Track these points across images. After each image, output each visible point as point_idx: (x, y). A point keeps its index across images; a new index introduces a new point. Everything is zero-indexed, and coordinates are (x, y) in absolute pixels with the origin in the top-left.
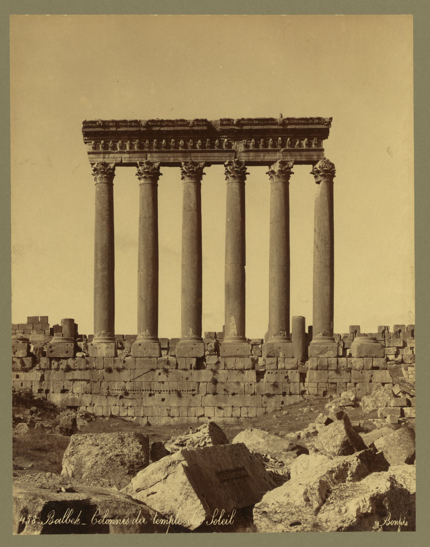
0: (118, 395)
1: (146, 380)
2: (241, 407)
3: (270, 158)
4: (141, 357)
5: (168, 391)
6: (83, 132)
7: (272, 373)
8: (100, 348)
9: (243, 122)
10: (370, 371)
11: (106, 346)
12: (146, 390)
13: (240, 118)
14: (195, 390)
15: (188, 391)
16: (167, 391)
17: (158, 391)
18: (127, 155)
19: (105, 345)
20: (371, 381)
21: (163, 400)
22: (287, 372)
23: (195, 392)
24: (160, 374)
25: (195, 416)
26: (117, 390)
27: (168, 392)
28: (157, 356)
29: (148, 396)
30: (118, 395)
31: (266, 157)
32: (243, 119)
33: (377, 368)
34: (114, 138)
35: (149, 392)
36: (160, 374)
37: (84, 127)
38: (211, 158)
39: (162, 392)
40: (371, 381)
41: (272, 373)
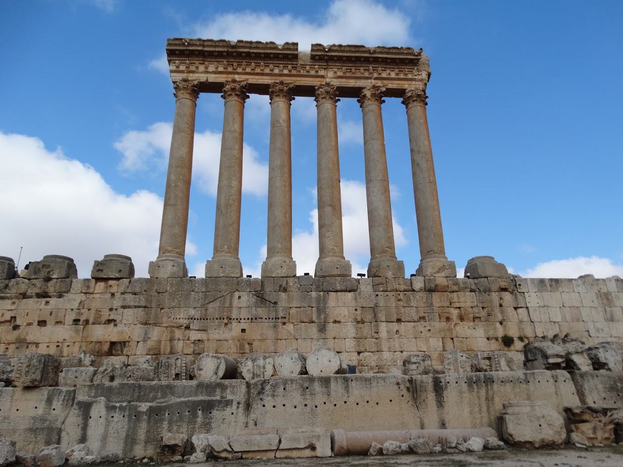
0: (182, 326)
2: (345, 339)
3: (361, 84)
5: (250, 318)
6: (167, 50)
8: (163, 266)
9: (335, 48)
10: (497, 293)
12: (220, 319)
13: (331, 44)
14: (285, 318)
15: (276, 318)
16: (248, 319)
17: (237, 319)
18: (212, 76)
19: (171, 263)
20: (501, 305)
21: (243, 331)
22: (399, 295)
23: (286, 320)
24: (239, 297)
26: (183, 318)
27: (250, 320)
28: (237, 276)
29: (223, 326)
30: (182, 326)
32: (334, 45)
33: (504, 290)
34: (200, 60)
36: (239, 297)
37: (169, 45)
38: (301, 82)
39: (242, 321)
40: (501, 305)
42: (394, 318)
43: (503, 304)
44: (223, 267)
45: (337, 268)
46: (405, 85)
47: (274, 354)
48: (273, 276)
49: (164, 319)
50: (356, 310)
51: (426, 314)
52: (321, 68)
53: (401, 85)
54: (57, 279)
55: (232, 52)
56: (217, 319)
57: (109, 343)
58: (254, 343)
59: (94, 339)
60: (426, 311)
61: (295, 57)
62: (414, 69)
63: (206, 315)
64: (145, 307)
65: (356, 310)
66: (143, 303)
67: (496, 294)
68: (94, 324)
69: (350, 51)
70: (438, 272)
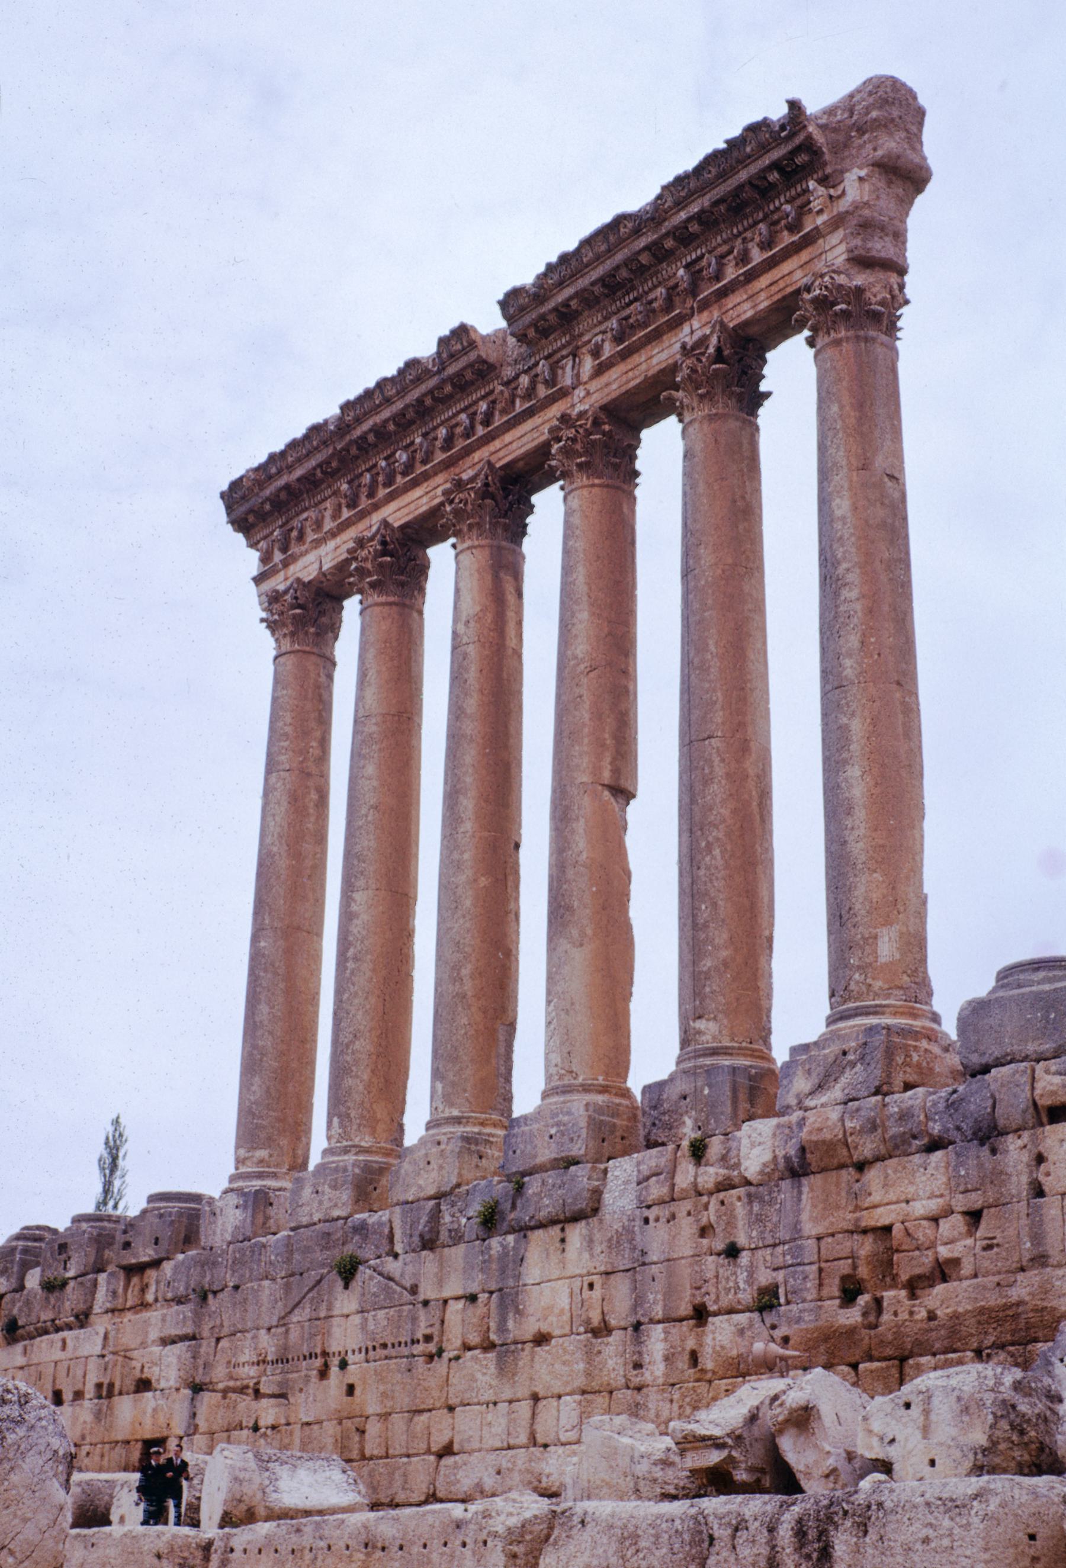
1: (314, 1315)
4: (306, 1226)
7: (657, 1220)
11: (236, 1202)
25: (428, 1451)
28: (344, 1214)
31: (655, 361)
35: (318, 1362)
38: (514, 445)
41: (657, 1220)
42: (685, 1308)
43: (1048, 1183)
44: (320, 1189)
45: (551, 1137)
46: (793, 273)
47: (405, 1460)
48: (410, 1199)
49: (220, 1368)
50: (591, 1286)
51: (782, 1273)
52: (563, 357)
53: (782, 284)
54: (75, 1278)
55: (346, 449)
56: (305, 1358)
57: (139, 1445)
58: (367, 1427)
59: (120, 1438)
60: (779, 1261)
61: (484, 370)
62: (806, 191)
63: (286, 1348)
64: (193, 1338)
65: (591, 1286)
66: (189, 1330)
67: (1020, 1143)
68: (120, 1394)
69: (598, 259)
70: (820, 1087)
